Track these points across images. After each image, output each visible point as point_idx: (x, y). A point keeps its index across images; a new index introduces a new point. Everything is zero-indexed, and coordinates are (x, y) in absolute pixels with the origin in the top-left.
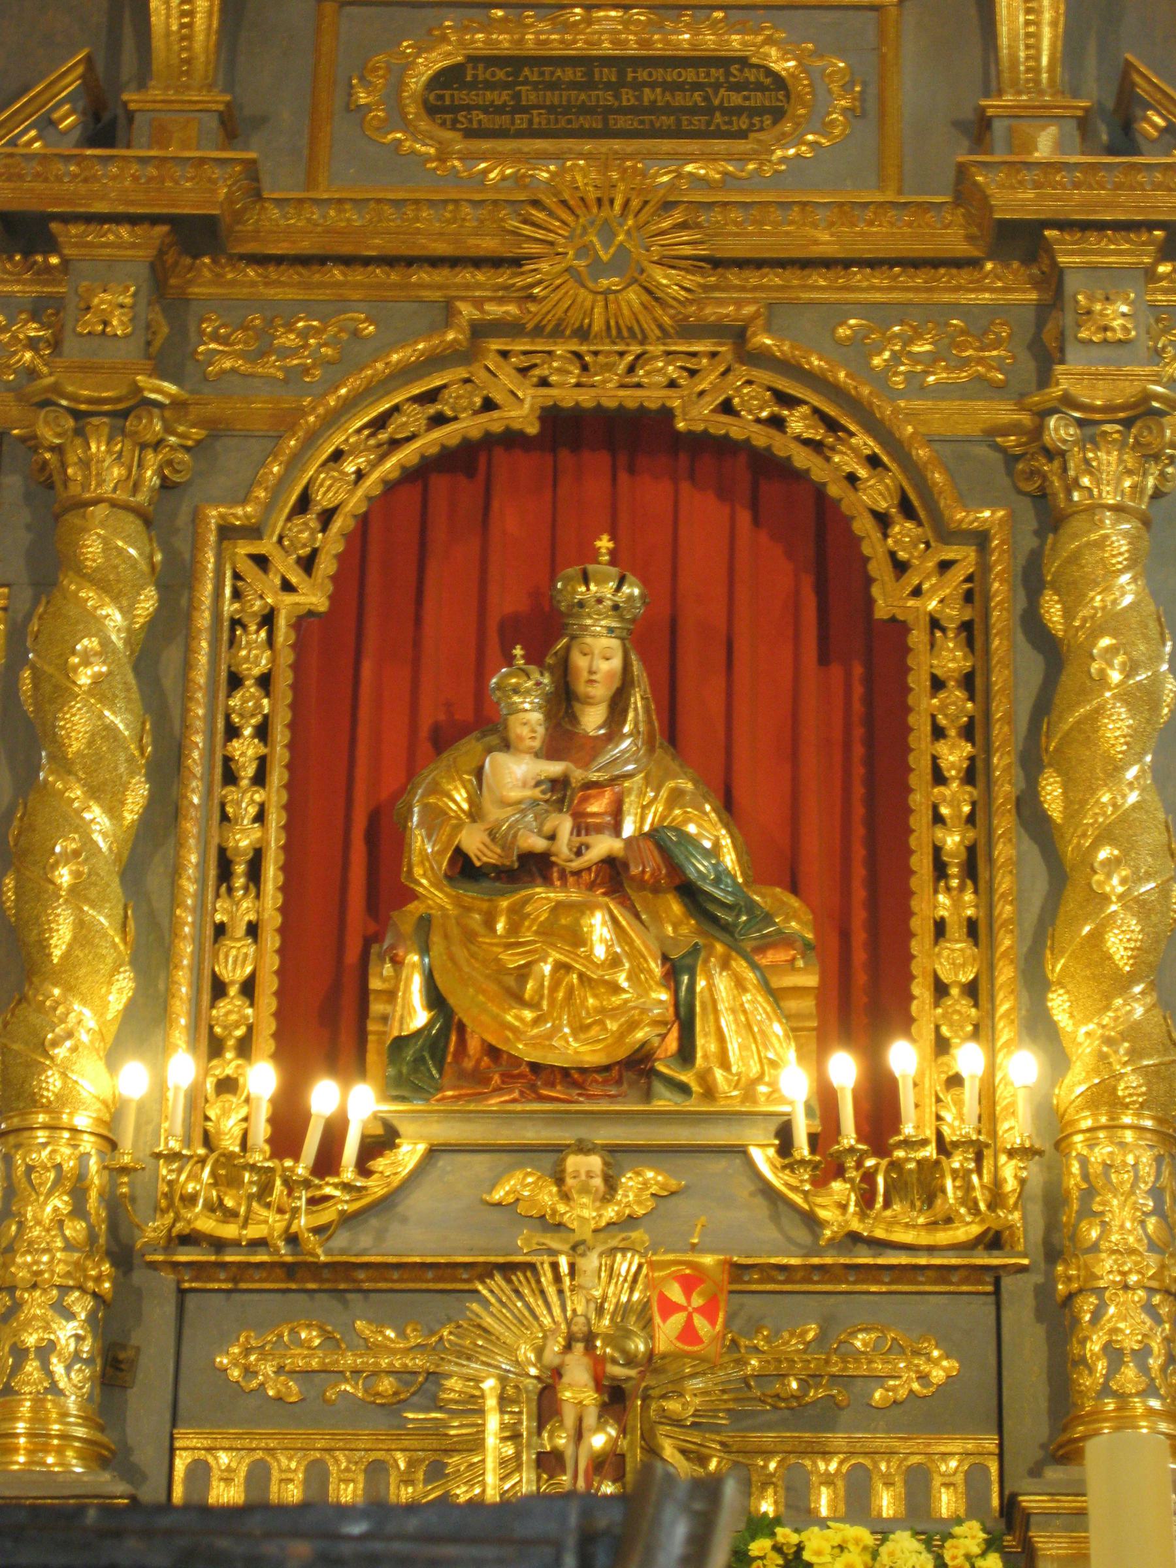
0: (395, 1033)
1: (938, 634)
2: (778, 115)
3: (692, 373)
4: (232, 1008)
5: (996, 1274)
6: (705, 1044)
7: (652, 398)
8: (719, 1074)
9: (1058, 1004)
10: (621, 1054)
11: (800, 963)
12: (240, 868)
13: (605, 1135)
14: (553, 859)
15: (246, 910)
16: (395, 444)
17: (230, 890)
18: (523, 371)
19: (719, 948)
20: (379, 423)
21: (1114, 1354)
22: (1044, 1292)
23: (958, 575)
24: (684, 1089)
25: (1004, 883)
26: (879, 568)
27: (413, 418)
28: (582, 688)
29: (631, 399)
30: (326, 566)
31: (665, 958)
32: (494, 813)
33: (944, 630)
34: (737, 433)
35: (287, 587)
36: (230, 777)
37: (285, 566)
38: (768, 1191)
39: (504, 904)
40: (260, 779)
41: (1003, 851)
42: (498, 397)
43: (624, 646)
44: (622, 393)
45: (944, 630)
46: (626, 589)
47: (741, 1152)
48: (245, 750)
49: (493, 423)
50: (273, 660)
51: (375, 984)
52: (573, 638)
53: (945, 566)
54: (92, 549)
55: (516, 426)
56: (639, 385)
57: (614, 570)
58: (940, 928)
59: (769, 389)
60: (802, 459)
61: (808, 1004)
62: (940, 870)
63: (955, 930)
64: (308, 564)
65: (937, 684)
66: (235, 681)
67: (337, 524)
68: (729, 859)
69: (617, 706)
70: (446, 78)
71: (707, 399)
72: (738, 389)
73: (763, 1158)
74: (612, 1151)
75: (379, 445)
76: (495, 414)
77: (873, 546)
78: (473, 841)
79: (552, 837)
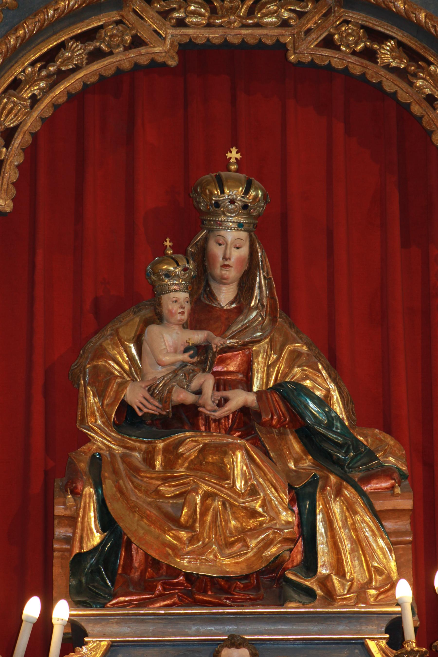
8: (336, 580)
10: (260, 566)
11: (398, 490)
14: (201, 409)
19: (333, 479)
28: (218, 271)
31: (291, 488)
34: (337, 64)
39: (160, 445)
42: (144, 35)
43: (250, 236)
44: (244, 32)
46: (252, 193)
51: (59, 510)
52: (210, 231)
55: (160, 59)
56: (257, 25)
57: (242, 176)
59: (362, 27)
71: (314, 36)
72: (338, 28)
75: (49, 76)
76: (143, 50)
79: (199, 392)
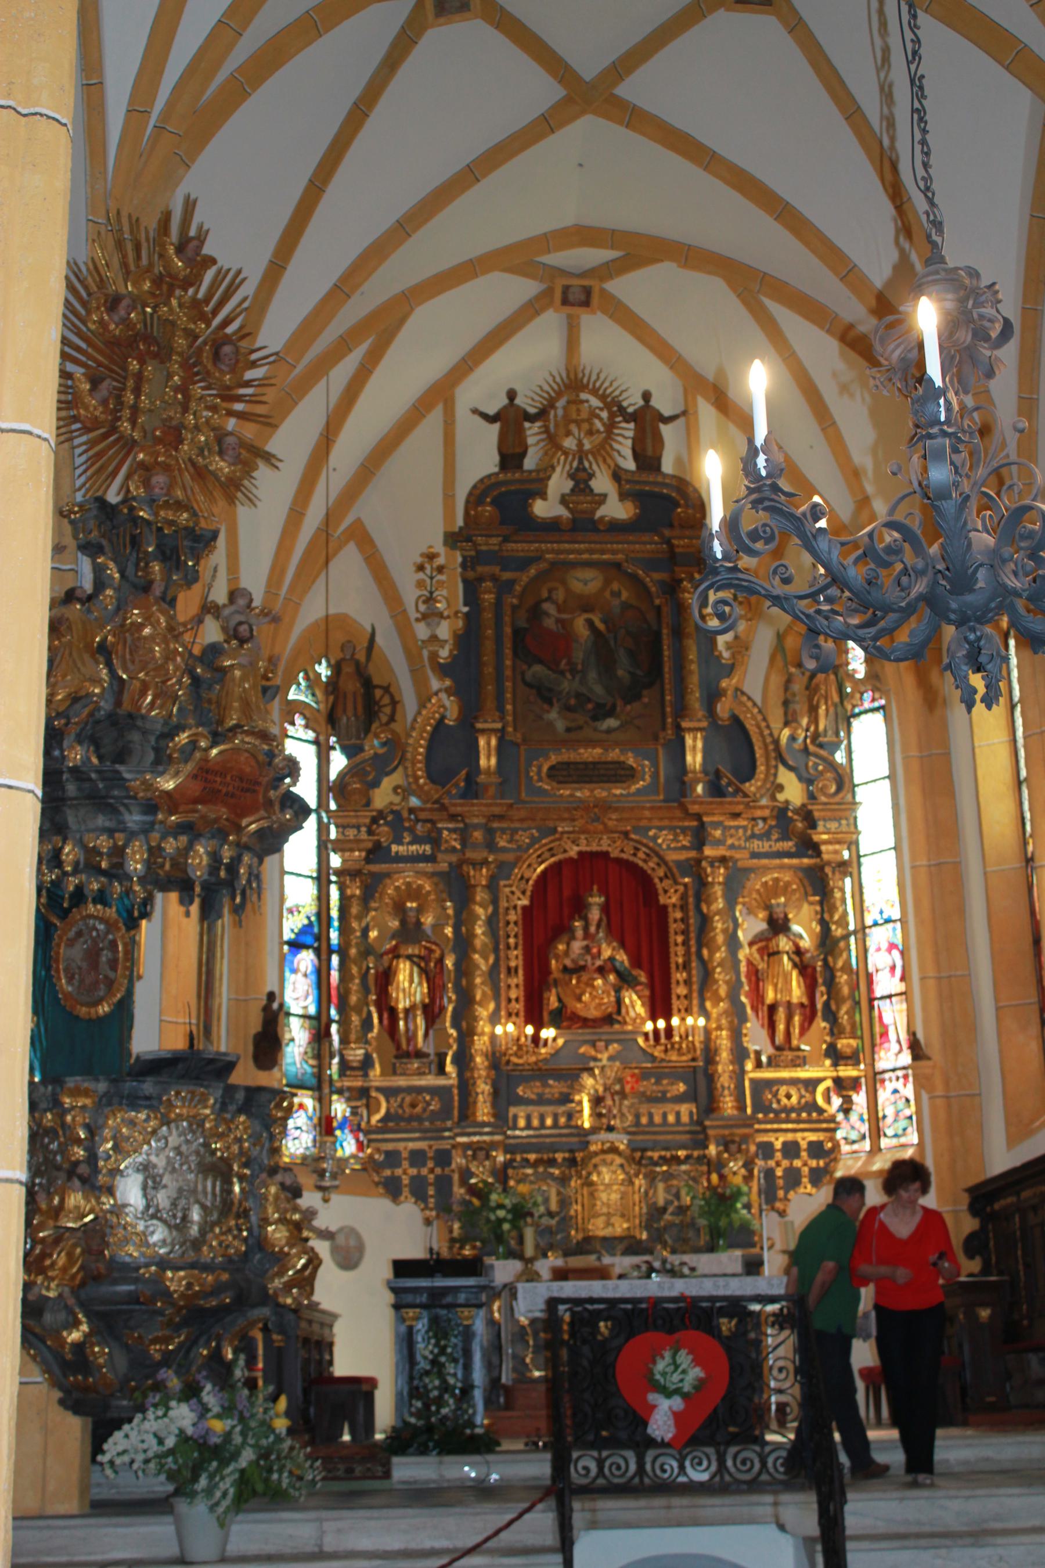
2: (633, 776)
5: (695, 1067)
6: (623, 1011)
7: (604, 848)
9: (708, 1005)
13: (604, 1037)
15: (515, 981)
20: (539, 856)
21: (723, 1087)
22: (706, 1070)
23: (679, 894)
24: (619, 1022)
25: (694, 972)
26: (660, 891)
27: (547, 855)
29: (599, 849)
30: (528, 893)
32: (573, 956)
37: (518, 894)
38: (641, 1048)
41: (694, 964)
48: (512, 941)
49: (566, 855)
54: (478, 898)
61: (646, 1000)
64: (524, 893)
66: (508, 923)
67: (531, 882)
68: (626, 963)
69: (598, 926)
70: (552, 768)
73: (641, 1041)
77: (659, 886)
78: (568, 962)
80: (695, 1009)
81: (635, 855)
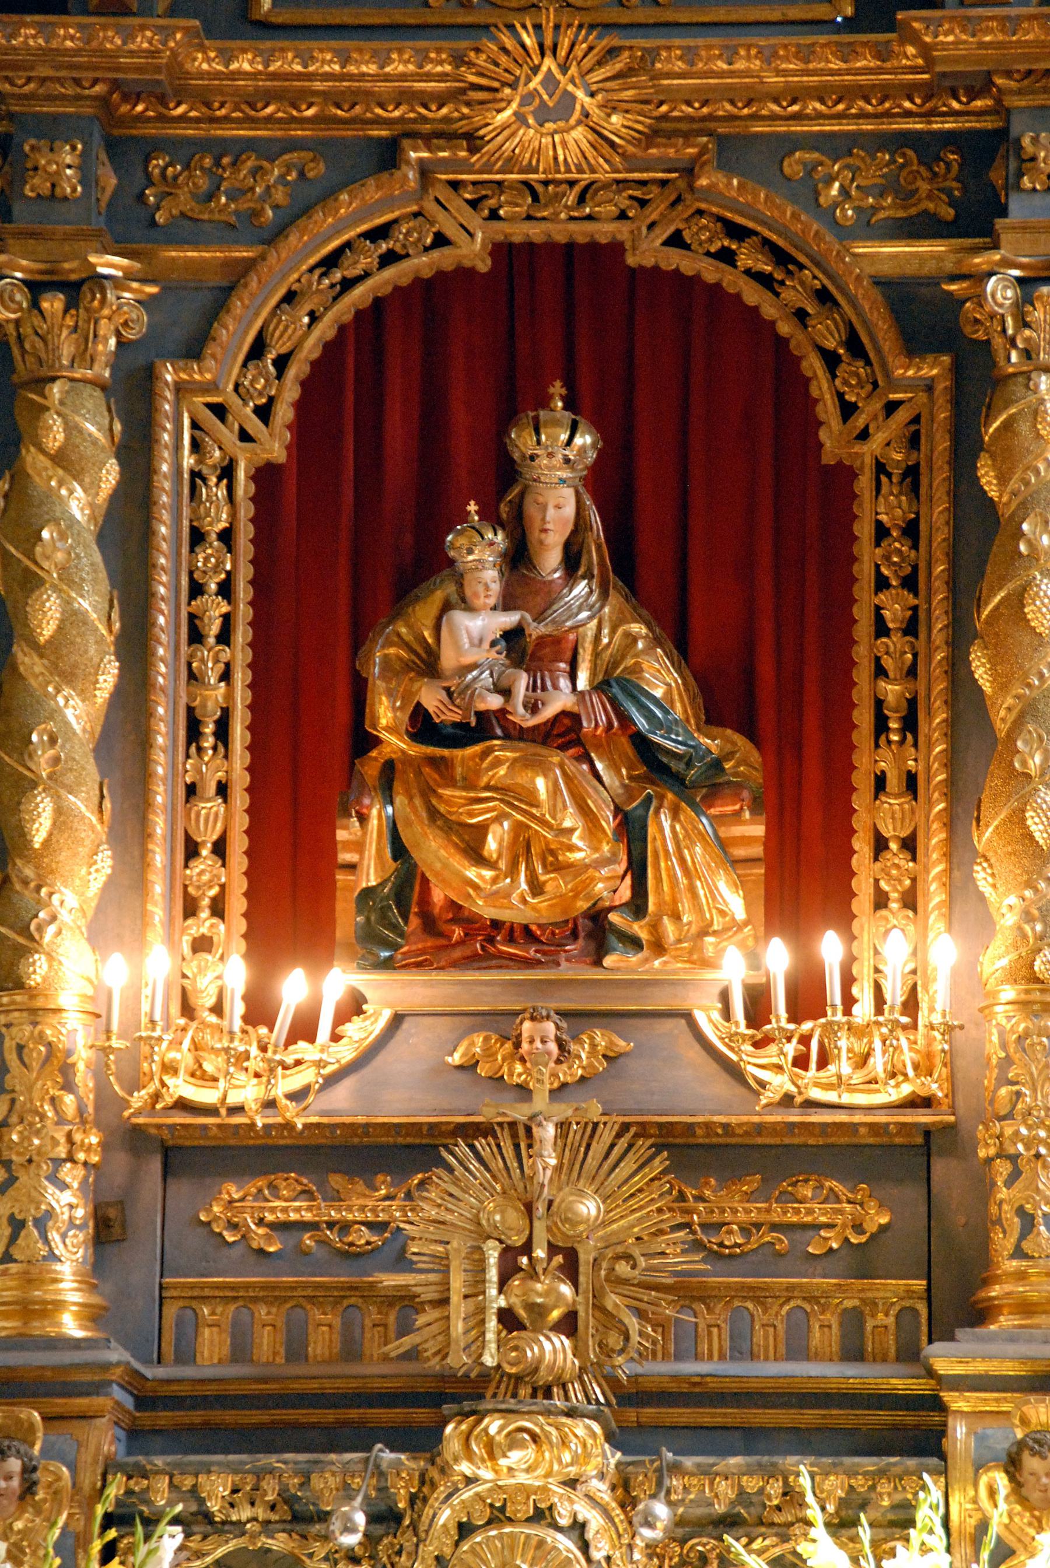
0: (364, 885)
1: (884, 479)
3: (643, 203)
4: (205, 863)
7: (605, 231)
11: (747, 815)
12: (209, 729)
14: (510, 717)
16: (347, 284)
17: (200, 750)
18: (474, 204)
19: (670, 796)
20: (331, 262)
24: (635, 944)
26: (828, 410)
29: (581, 232)
30: (284, 413)
33: (889, 475)
35: (245, 436)
36: (196, 637)
37: (245, 413)
40: (224, 637)
42: (451, 231)
44: (573, 226)
45: (889, 475)
47: (688, 1017)
49: (443, 259)
50: (233, 515)
53: (891, 407)
55: (467, 263)
56: (590, 218)
57: (568, 416)
58: (880, 783)
60: (752, 295)
62: (881, 726)
63: (893, 782)
64: (264, 413)
65: (881, 532)
67: (295, 371)
71: (657, 230)
74: (564, 1014)
76: (446, 250)
77: (822, 387)
78: (431, 698)
80: (935, 895)
81: (726, 257)
